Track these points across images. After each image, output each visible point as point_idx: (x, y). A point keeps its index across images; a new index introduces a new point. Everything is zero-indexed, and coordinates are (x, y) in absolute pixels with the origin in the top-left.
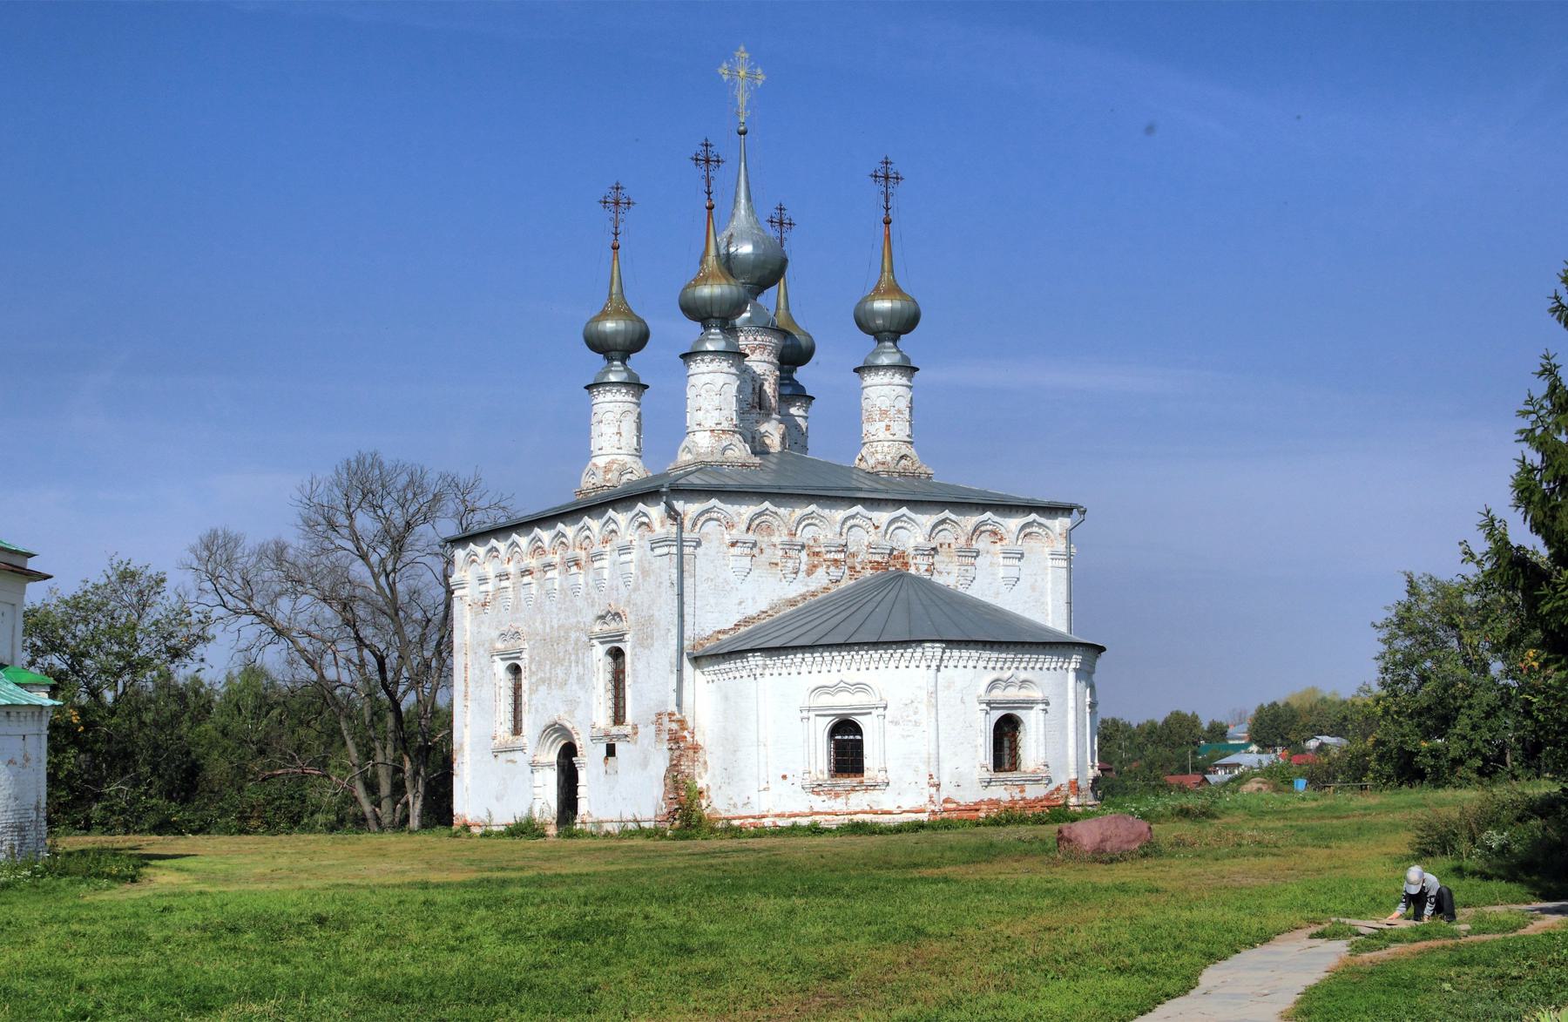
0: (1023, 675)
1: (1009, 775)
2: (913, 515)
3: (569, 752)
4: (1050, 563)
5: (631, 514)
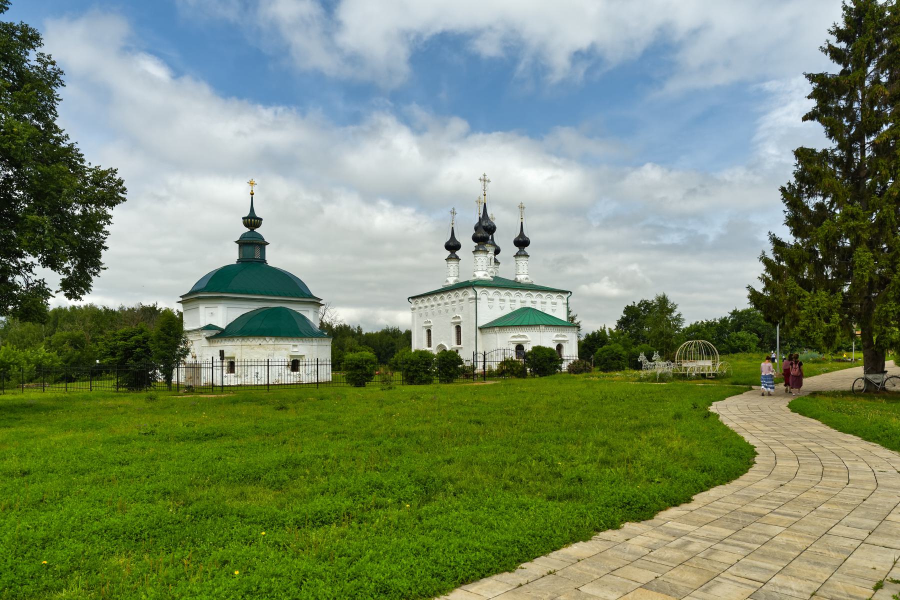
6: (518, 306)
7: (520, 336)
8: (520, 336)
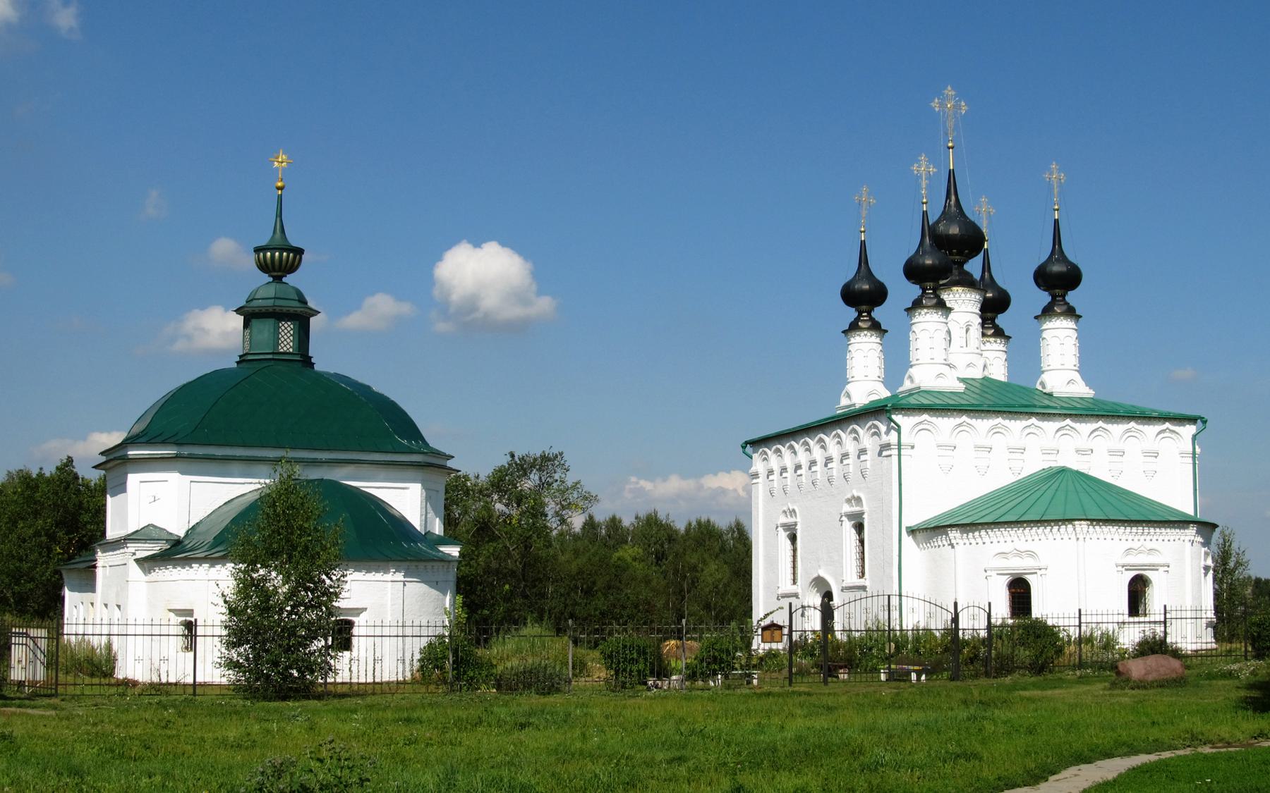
0: (1149, 545)
1: (1142, 619)
2: (1073, 424)
3: (828, 596)
6: (1033, 464)
7: (1019, 553)
8: (1019, 553)
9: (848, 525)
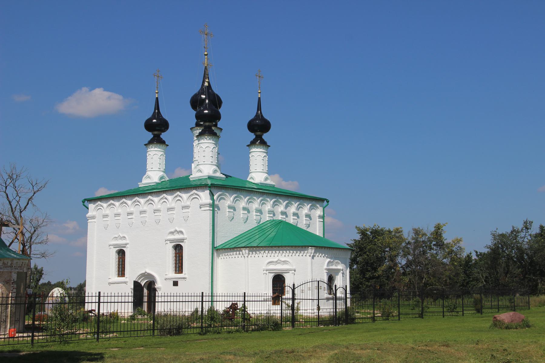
4: (318, 220)
5: (189, 194)
9: (170, 246)
